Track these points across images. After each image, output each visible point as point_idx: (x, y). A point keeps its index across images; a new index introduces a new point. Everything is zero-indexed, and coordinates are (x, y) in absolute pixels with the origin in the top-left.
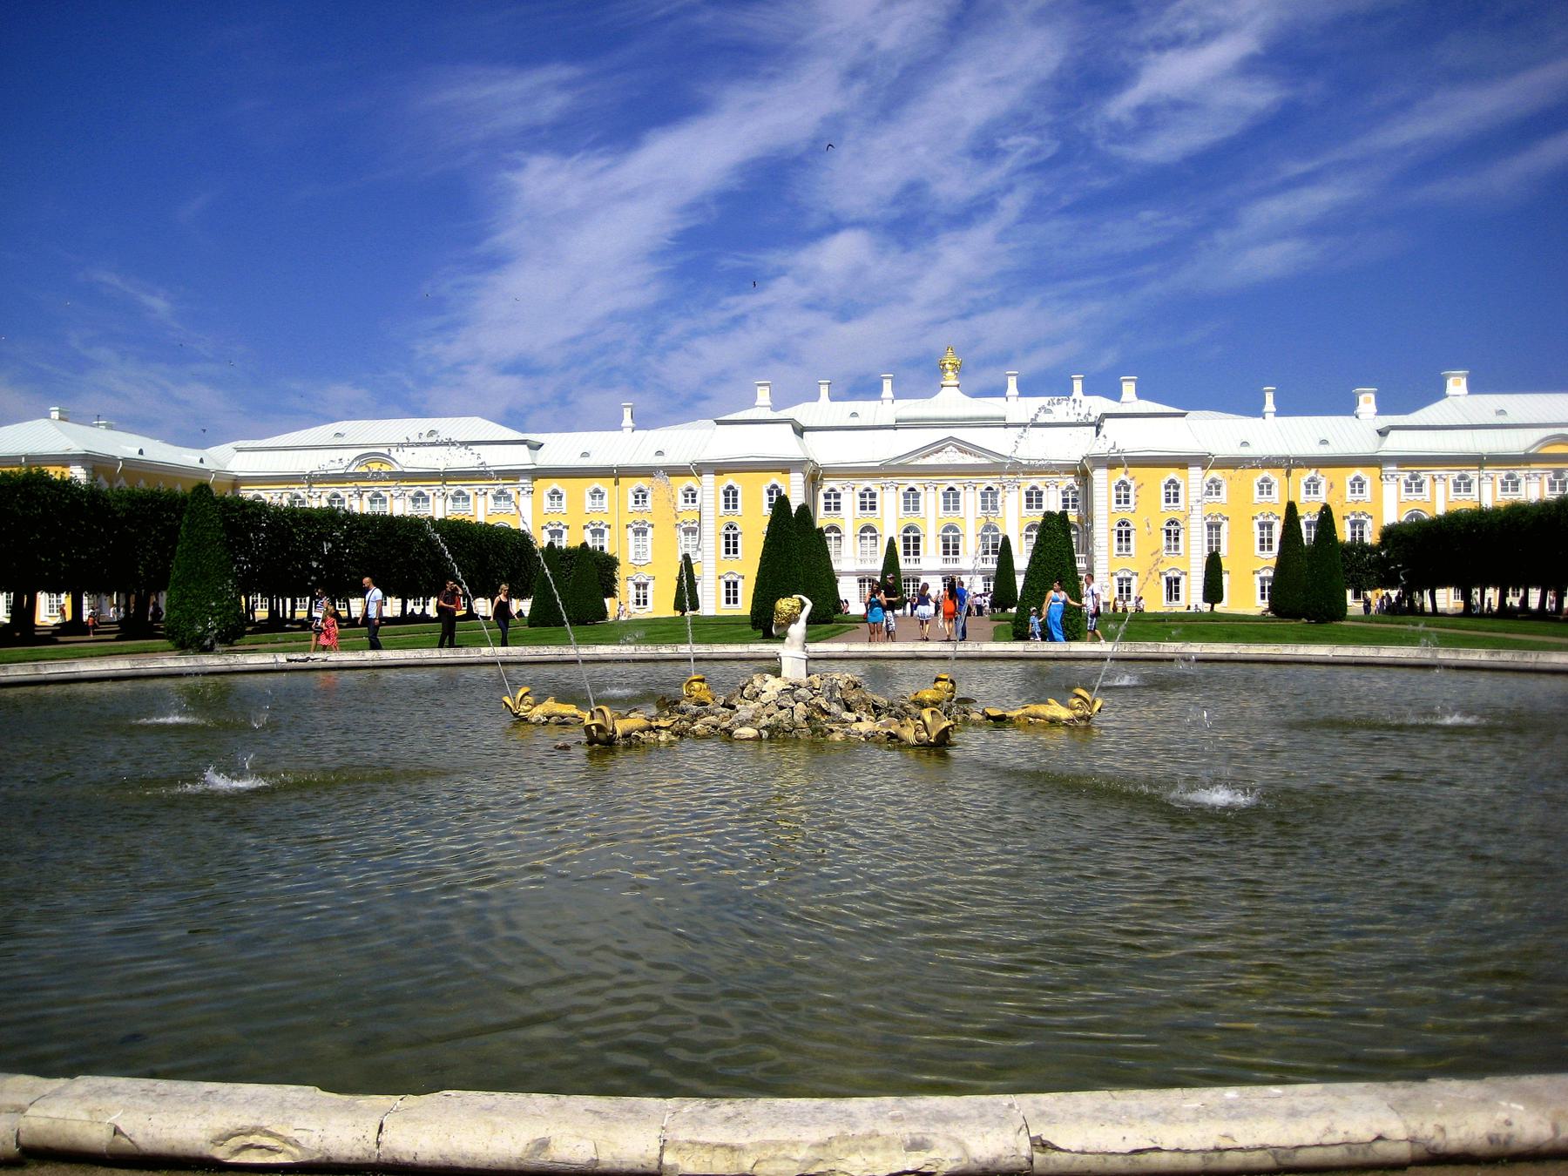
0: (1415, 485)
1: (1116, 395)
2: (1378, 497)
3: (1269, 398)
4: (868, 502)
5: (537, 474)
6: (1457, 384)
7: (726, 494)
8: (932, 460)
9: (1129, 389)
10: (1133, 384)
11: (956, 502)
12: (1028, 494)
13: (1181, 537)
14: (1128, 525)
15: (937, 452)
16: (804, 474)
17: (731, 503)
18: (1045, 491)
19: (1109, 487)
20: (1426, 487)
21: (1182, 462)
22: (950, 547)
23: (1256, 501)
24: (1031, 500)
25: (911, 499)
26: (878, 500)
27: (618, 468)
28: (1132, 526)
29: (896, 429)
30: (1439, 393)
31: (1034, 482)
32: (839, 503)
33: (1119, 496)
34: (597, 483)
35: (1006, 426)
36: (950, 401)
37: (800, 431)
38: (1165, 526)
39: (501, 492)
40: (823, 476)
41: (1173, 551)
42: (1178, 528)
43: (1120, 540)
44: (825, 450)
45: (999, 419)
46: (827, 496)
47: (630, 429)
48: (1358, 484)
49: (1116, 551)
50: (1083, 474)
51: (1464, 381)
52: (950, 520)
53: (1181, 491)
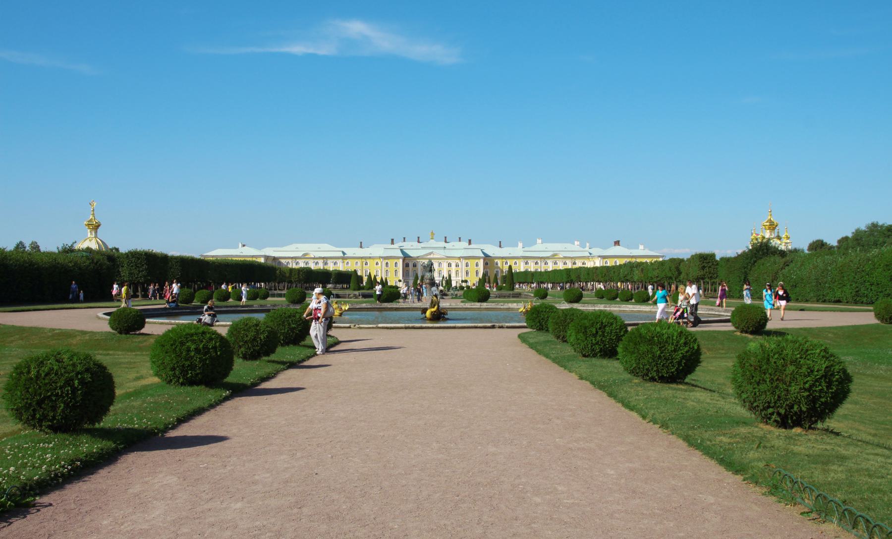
2: (520, 265)
6: (539, 241)
12: (449, 264)
30: (535, 243)
34: (357, 260)
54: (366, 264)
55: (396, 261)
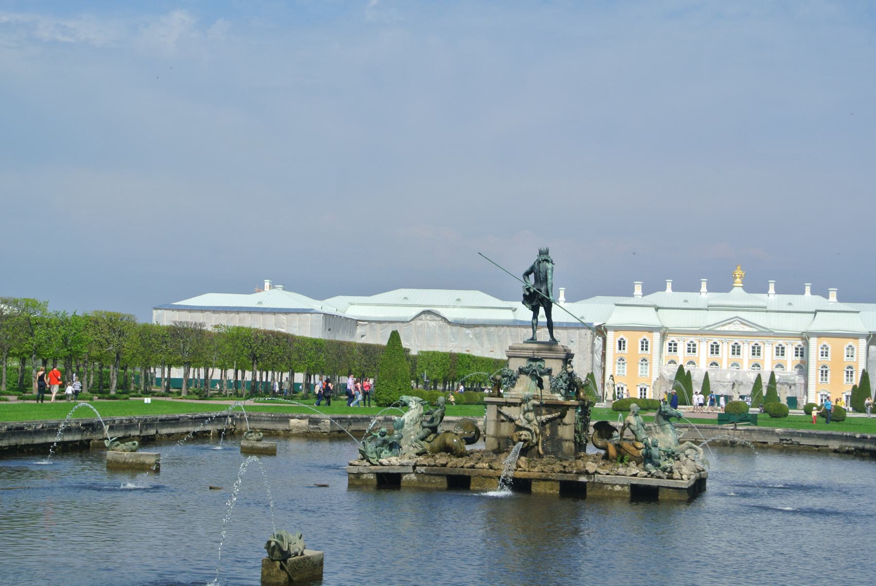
4: (692, 349)
8: (726, 328)
9: (833, 296)
12: (777, 348)
14: (827, 368)
15: (729, 323)
16: (660, 333)
18: (786, 347)
19: (818, 348)
21: (856, 337)
24: (779, 352)
26: (697, 347)
29: (708, 310)
33: (822, 352)
35: (767, 311)
36: (737, 295)
37: (657, 309)
38: (846, 369)
40: (669, 333)
41: (849, 382)
42: (852, 370)
43: (822, 375)
44: (670, 319)
46: (670, 344)
49: (820, 381)
50: (805, 337)
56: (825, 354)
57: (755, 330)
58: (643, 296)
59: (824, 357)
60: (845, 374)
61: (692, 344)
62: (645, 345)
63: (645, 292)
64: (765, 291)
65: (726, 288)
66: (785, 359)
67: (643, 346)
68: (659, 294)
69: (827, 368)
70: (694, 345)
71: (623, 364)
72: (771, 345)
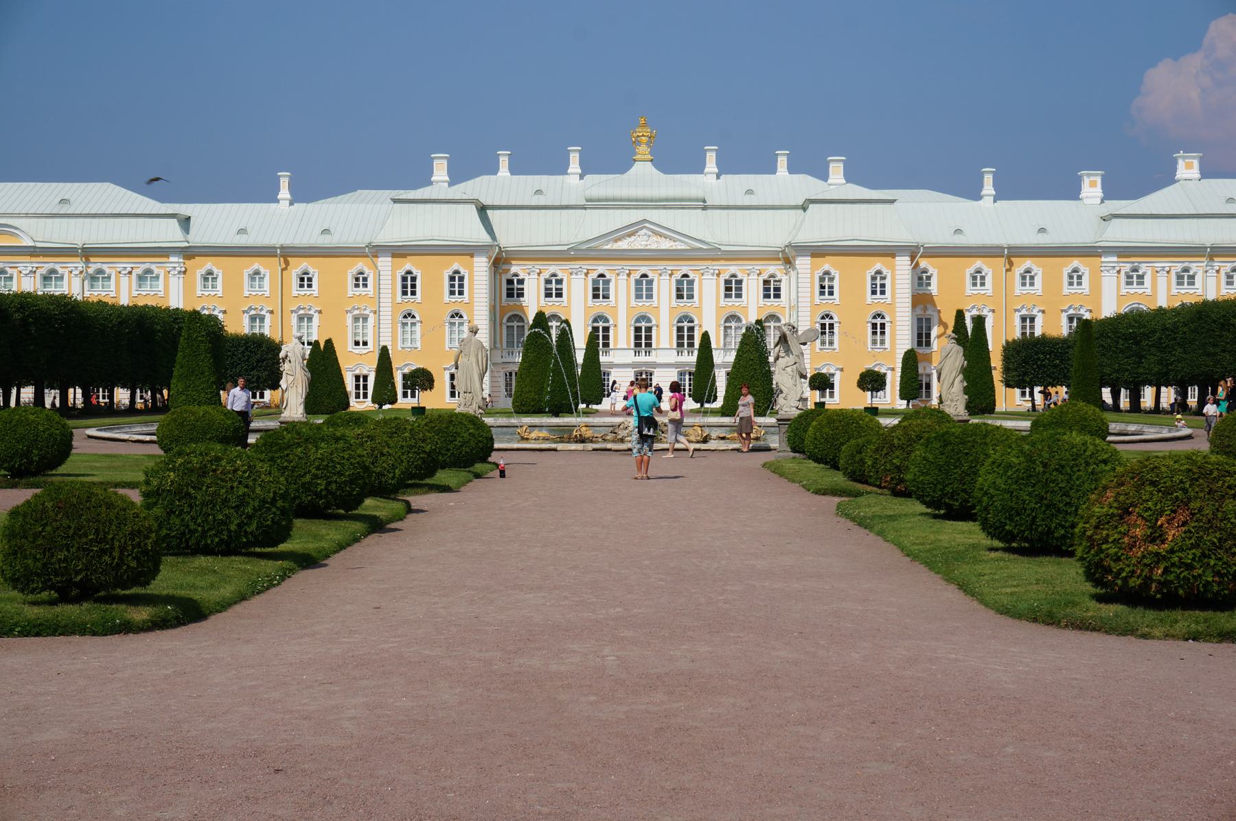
0: (1134, 277)
1: (824, 176)
3: (988, 180)
5: (189, 253)
6: (1188, 169)
7: (452, 279)
8: (623, 245)
9: (836, 171)
10: (841, 165)
11: (650, 290)
13: (887, 330)
15: (629, 236)
16: (490, 258)
17: (409, 290)
19: (812, 278)
20: (1147, 279)
21: (889, 252)
22: (643, 338)
23: (968, 292)
25: (644, 287)
26: (564, 286)
27: (282, 248)
28: (836, 319)
29: (585, 208)
30: (1167, 178)
31: (733, 269)
32: (523, 289)
33: (822, 287)
34: (257, 264)
35: (705, 208)
39: (149, 271)
41: (878, 346)
45: (697, 200)
47: (288, 202)
48: (1075, 277)
51: (1196, 163)
52: (643, 311)
53: (888, 282)
54: (305, 280)
55: (456, 264)
56: (825, 289)
57: (683, 247)
58: (451, 184)
59: (827, 296)
60: (870, 330)
61: (554, 279)
62: (457, 283)
63: (456, 177)
64: (699, 168)
65: (621, 164)
66: (744, 304)
67: (452, 286)
68: (485, 179)
69: (831, 318)
70: (559, 282)
71: (413, 324)
72: (715, 277)
